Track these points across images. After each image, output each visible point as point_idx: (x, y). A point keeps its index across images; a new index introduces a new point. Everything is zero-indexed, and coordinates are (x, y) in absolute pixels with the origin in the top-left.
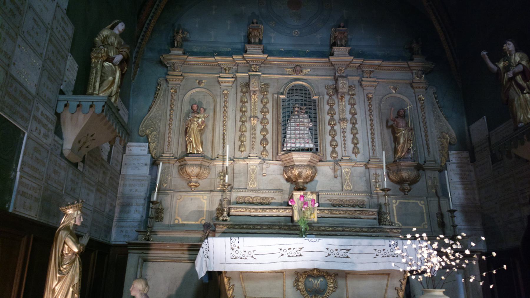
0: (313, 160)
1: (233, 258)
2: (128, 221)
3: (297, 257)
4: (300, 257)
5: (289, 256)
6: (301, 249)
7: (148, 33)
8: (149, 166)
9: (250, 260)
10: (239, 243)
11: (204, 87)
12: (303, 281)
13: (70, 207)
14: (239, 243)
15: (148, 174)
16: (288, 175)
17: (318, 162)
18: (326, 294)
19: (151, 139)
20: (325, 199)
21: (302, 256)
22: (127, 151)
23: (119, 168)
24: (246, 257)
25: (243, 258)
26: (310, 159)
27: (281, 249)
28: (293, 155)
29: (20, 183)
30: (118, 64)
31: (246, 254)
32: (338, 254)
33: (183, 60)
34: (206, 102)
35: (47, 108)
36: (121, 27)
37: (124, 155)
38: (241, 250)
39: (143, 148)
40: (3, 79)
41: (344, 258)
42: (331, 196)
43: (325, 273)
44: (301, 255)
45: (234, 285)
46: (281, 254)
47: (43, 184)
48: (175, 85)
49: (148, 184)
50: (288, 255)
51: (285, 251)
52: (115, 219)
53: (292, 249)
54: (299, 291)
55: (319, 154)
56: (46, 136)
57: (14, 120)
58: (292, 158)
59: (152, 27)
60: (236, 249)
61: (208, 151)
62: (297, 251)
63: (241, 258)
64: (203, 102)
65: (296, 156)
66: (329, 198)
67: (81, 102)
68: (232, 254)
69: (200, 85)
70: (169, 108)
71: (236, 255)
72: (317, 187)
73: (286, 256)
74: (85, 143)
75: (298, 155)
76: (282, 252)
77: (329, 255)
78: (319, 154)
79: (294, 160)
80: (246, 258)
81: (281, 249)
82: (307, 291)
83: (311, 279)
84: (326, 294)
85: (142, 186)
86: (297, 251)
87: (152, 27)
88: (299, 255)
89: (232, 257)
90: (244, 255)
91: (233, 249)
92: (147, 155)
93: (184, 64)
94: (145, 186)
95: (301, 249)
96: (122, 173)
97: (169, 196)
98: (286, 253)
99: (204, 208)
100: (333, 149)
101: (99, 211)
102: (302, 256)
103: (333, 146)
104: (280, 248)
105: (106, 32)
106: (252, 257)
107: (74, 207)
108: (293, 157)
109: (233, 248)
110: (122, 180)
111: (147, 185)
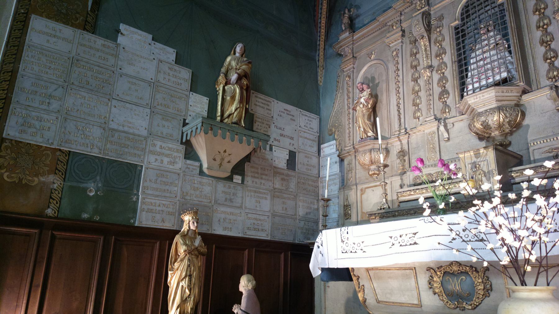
0: (503, 96)
1: (344, 251)
2: (330, 221)
3: (411, 246)
4: (415, 245)
5: (401, 245)
6: (415, 234)
7: (323, 31)
8: (338, 164)
9: (360, 253)
10: (347, 233)
11: (376, 58)
12: (438, 280)
13: (186, 214)
14: (347, 233)
15: (338, 171)
16: (474, 131)
17: (521, 96)
18: (475, 300)
19: (337, 136)
20: (541, 150)
21: (417, 244)
22: (322, 154)
23: (317, 172)
24: (355, 250)
25: (352, 252)
26: (496, 96)
27: (391, 237)
28: (468, 100)
29: (143, 203)
30: (235, 82)
31: (355, 246)
32: (467, 236)
33: (351, 41)
34: (379, 74)
35: (166, 142)
36: (239, 48)
37: (320, 158)
38: (350, 242)
39: (332, 147)
40: (101, 134)
41: (477, 243)
42: (549, 144)
43: (468, 268)
44: (415, 243)
45: (363, 286)
46: (392, 244)
47: (179, 200)
48: (349, 71)
49: (339, 182)
50: (400, 244)
51: (396, 239)
52: (320, 221)
53: (404, 236)
54: (437, 295)
55: (518, 83)
56: (173, 163)
57: (124, 159)
58: (469, 106)
59: (323, 23)
60: (346, 241)
61: (385, 130)
62: (410, 238)
63: (351, 252)
64: (376, 77)
65: (473, 101)
66: (547, 149)
67: (213, 126)
68: (343, 248)
69: (371, 58)
70: (346, 97)
71: (347, 249)
72: (528, 136)
73: (397, 245)
74: (223, 159)
75: (475, 97)
76: (392, 241)
77: (454, 239)
78: (518, 83)
79: (473, 106)
80: (356, 252)
81: (391, 237)
82: (447, 295)
83: (448, 277)
84: (475, 300)
85: (335, 185)
86: (410, 238)
87: (323, 23)
88: (413, 243)
89: (343, 251)
90: (353, 248)
91: (343, 242)
92: (336, 152)
93: (353, 43)
94: (337, 184)
95: (415, 234)
96: (320, 176)
97: (353, 190)
98: (397, 242)
99: (325, 196)
100: (549, 66)
101: (284, 215)
102: (417, 244)
103: (548, 61)
104: (390, 236)
105: (229, 59)
106: (362, 250)
107: (190, 213)
108: (469, 102)
109: (343, 240)
110: (321, 182)
111: (338, 183)
